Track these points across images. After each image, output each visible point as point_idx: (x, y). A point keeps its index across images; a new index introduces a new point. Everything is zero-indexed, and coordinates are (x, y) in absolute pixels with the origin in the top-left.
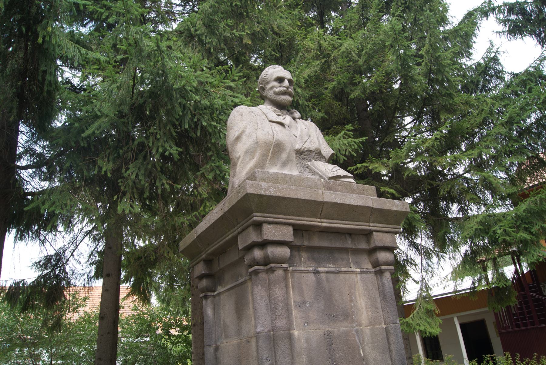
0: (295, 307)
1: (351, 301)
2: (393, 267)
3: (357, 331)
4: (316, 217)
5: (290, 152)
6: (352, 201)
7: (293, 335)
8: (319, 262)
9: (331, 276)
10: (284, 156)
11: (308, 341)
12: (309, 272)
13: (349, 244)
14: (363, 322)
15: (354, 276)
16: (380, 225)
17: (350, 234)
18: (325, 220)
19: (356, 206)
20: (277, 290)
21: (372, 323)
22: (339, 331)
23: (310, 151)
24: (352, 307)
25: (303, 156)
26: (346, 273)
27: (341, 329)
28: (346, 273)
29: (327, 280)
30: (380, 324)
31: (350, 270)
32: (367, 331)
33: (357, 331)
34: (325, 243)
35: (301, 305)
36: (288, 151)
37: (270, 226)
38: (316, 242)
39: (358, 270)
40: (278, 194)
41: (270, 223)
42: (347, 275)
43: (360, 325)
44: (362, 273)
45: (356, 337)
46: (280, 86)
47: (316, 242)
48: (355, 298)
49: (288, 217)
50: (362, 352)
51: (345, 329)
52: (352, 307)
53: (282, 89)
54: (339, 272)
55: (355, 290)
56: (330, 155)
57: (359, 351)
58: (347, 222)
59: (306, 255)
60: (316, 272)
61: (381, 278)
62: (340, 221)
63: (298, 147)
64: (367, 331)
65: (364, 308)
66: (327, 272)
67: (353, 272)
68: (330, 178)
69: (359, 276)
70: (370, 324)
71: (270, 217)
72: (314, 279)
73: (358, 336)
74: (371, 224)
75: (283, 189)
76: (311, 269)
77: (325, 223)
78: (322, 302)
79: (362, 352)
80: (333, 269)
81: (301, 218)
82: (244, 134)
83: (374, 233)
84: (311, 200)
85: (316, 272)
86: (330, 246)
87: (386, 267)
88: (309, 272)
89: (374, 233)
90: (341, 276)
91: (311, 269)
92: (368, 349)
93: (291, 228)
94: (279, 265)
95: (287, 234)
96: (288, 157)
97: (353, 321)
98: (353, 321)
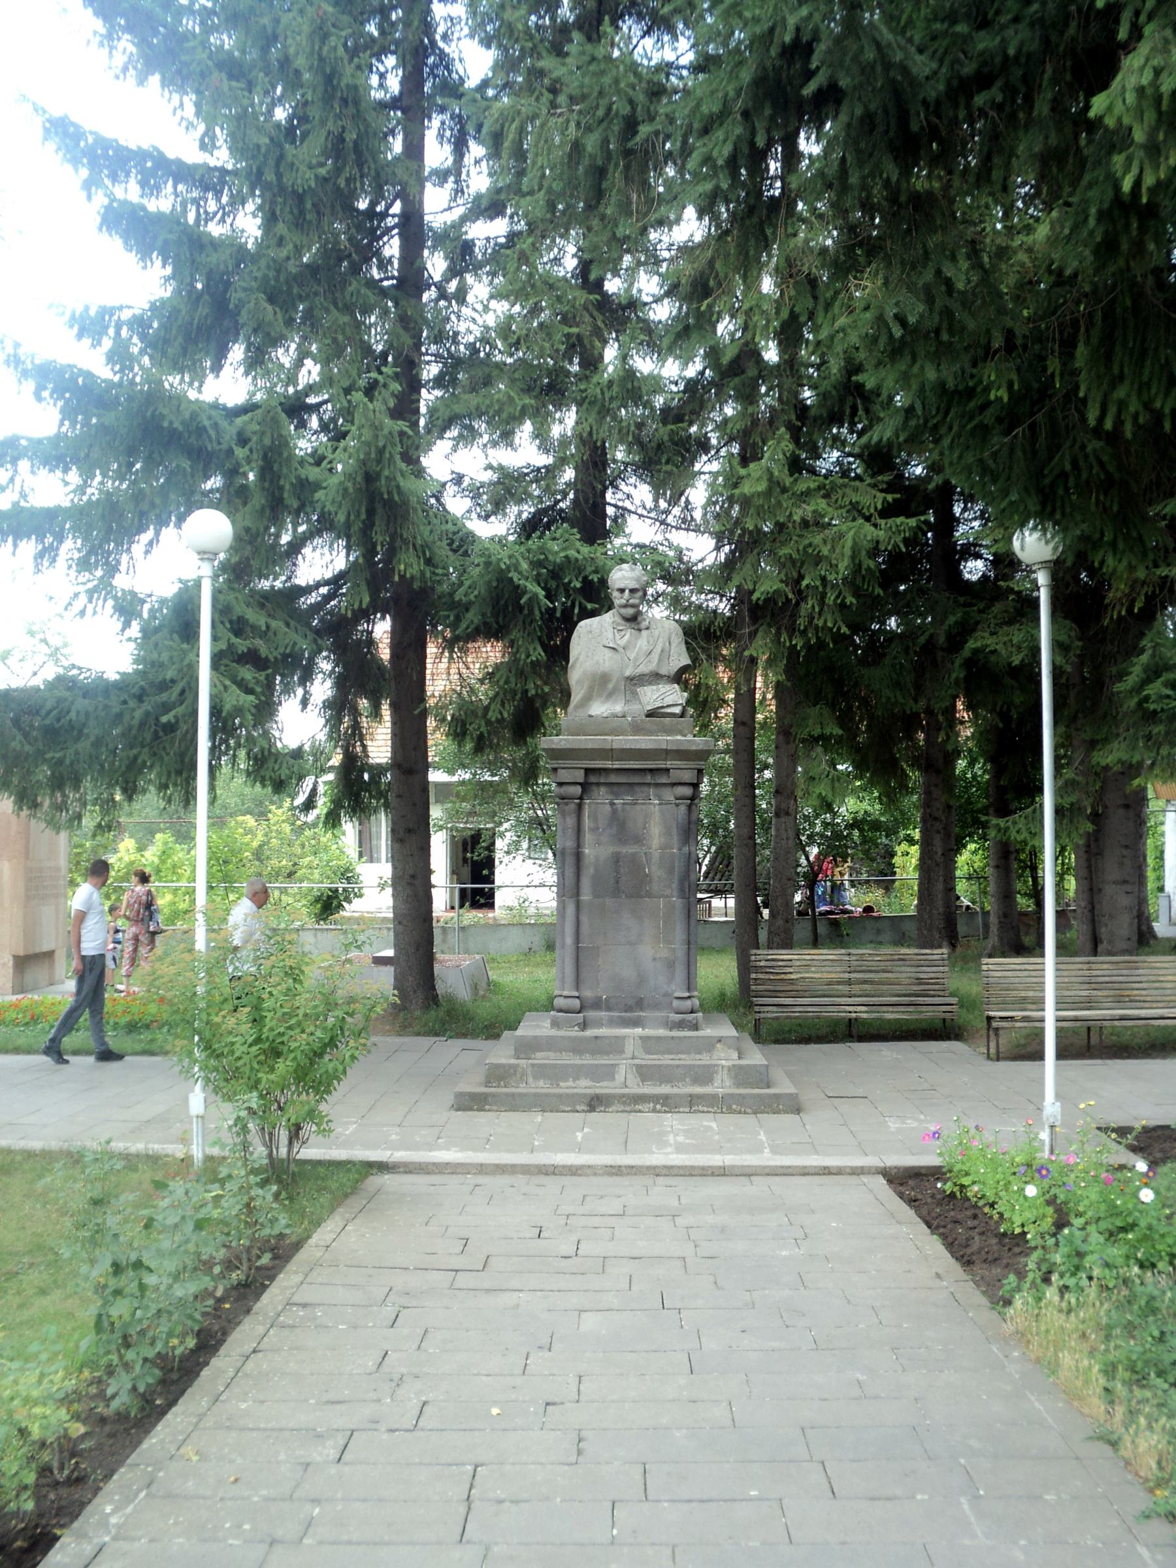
8: (617, 796)
10: (610, 686)
13: (648, 779)
21: (663, 847)
32: (656, 855)
35: (594, 830)
38: (613, 778)
47: (613, 778)
53: (623, 601)
60: (612, 804)
63: (628, 673)
77: (617, 765)
92: (654, 868)
95: (580, 776)
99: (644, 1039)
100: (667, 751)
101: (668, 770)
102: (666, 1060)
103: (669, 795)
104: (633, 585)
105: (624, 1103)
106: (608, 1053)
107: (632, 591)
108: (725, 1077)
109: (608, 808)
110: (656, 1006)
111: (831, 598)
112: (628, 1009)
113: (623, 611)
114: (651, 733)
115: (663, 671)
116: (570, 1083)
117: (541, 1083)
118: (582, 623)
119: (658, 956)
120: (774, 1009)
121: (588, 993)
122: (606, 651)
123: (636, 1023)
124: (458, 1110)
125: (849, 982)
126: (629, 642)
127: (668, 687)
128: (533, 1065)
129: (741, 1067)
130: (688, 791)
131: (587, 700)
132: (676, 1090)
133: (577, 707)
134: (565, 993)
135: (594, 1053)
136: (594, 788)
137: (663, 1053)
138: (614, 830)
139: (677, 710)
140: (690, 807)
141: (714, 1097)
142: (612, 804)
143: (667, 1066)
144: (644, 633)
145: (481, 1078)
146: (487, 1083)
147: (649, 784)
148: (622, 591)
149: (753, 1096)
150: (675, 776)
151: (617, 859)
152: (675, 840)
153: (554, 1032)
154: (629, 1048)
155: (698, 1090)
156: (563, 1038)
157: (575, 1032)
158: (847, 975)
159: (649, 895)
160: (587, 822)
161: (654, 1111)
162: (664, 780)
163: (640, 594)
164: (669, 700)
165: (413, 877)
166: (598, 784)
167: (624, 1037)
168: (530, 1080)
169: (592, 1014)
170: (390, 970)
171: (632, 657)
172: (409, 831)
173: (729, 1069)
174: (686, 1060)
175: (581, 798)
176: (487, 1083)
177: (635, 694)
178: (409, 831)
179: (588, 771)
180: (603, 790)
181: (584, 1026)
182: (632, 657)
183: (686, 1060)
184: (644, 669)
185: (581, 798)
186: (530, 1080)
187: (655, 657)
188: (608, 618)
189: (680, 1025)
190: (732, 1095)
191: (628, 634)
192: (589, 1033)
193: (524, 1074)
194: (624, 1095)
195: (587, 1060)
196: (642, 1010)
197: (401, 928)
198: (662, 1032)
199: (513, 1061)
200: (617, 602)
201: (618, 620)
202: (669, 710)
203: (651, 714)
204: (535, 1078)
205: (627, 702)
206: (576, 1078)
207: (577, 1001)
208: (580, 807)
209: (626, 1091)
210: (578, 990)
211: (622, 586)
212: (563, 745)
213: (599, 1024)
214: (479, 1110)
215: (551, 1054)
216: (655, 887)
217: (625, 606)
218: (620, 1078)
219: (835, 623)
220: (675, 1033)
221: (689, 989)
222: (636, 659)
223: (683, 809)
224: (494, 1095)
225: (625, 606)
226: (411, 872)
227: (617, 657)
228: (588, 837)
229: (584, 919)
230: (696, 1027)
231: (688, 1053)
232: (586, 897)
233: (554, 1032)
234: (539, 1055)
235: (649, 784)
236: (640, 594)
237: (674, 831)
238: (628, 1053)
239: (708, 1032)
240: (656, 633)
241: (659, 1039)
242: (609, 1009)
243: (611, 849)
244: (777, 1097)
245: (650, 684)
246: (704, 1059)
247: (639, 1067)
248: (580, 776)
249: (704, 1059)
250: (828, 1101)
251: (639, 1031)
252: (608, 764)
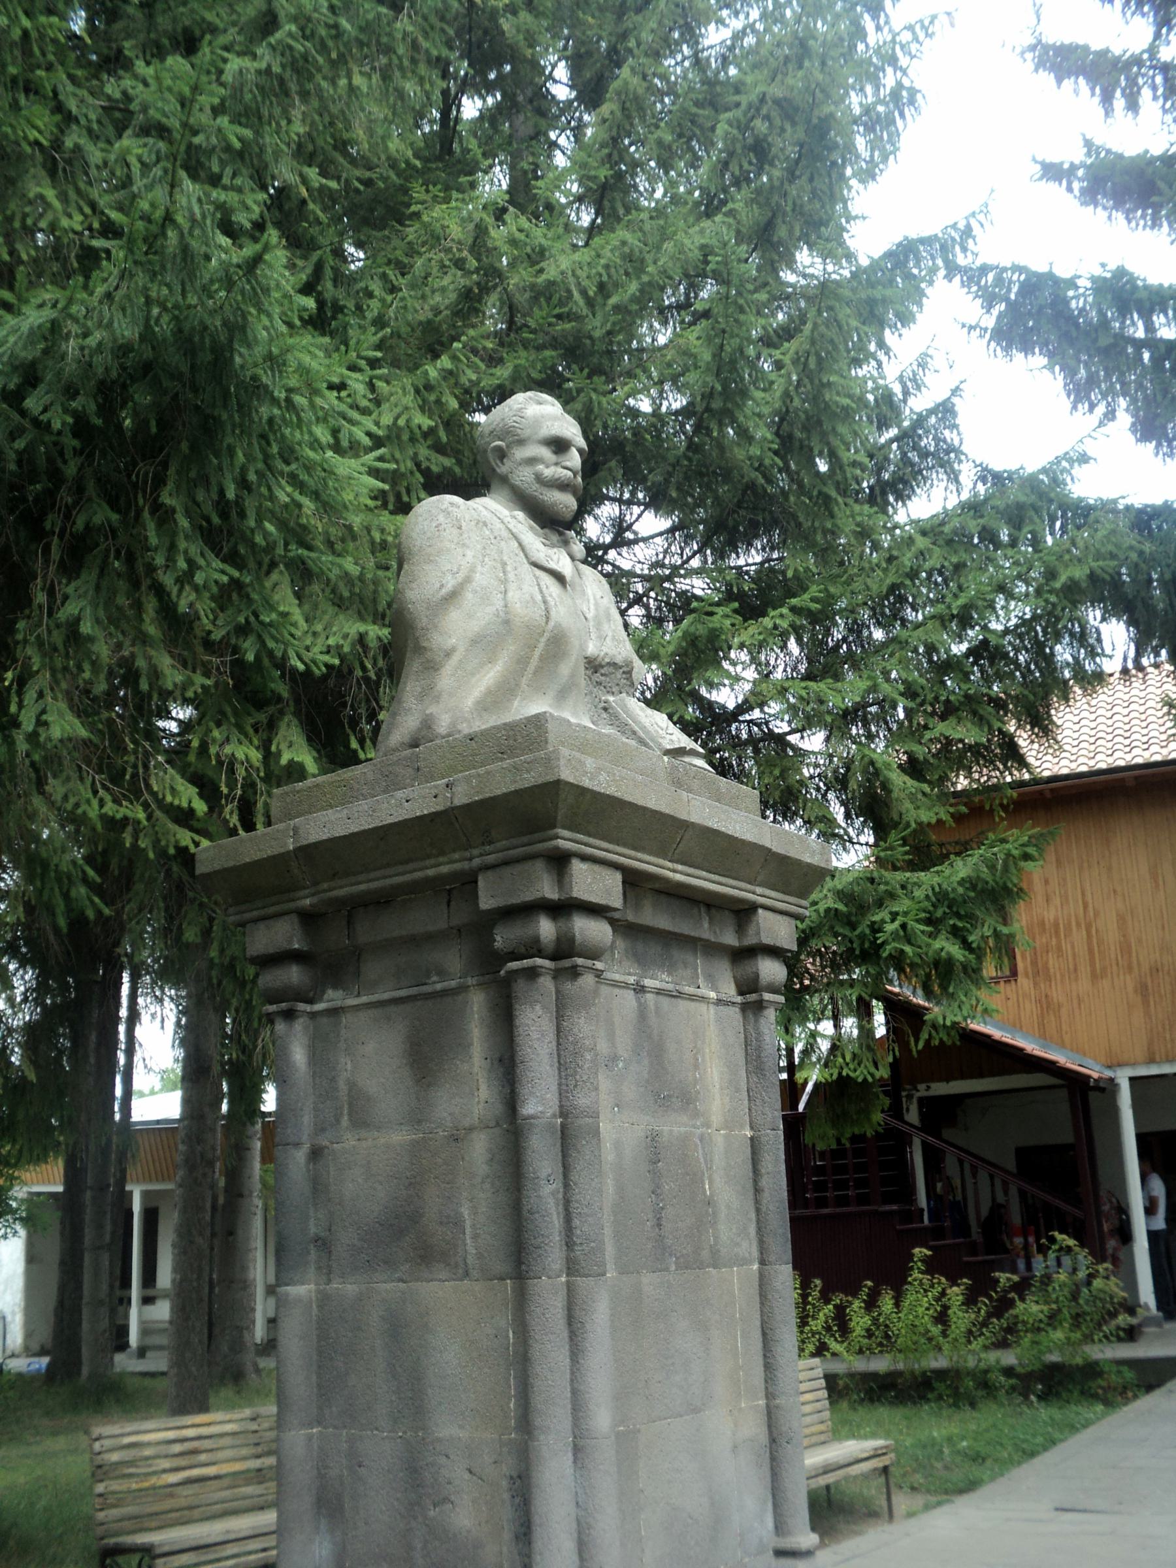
1: (696, 1067)
3: (702, 1138)
9: (665, 1001)
12: (626, 986)
13: (704, 930)
15: (703, 1007)
16: (773, 894)
17: (709, 906)
18: (680, 867)
19: (743, 842)
20: (582, 1021)
23: (615, 664)
24: (696, 1082)
25: (597, 677)
28: (692, 998)
30: (742, 1127)
31: (699, 992)
33: (702, 1138)
39: (713, 995)
40: (611, 791)
41: (584, 858)
44: (719, 1002)
46: (556, 464)
51: (683, 1129)
52: (696, 1082)
54: (679, 995)
57: (703, 1183)
58: (712, 877)
60: (640, 989)
61: (756, 1021)
63: (592, 649)
64: (719, 1139)
66: (659, 992)
67: (703, 999)
68: (668, 752)
69: (712, 1007)
71: (586, 844)
72: (634, 1003)
74: (759, 890)
75: (623, 778)
78: (646, 1062)
80: (670, 987)
82: (470, 587)
83: (760, 911)
85: (640, 989)
86: (671, 929)
88: (626, 986)
89: (760, 911)
90: (683, 1004)
91: (631, 980)
93: (618, 876)
94: (589, 963)
96: (572, 676)
97: (696, 1114)
98: (696, 1114)
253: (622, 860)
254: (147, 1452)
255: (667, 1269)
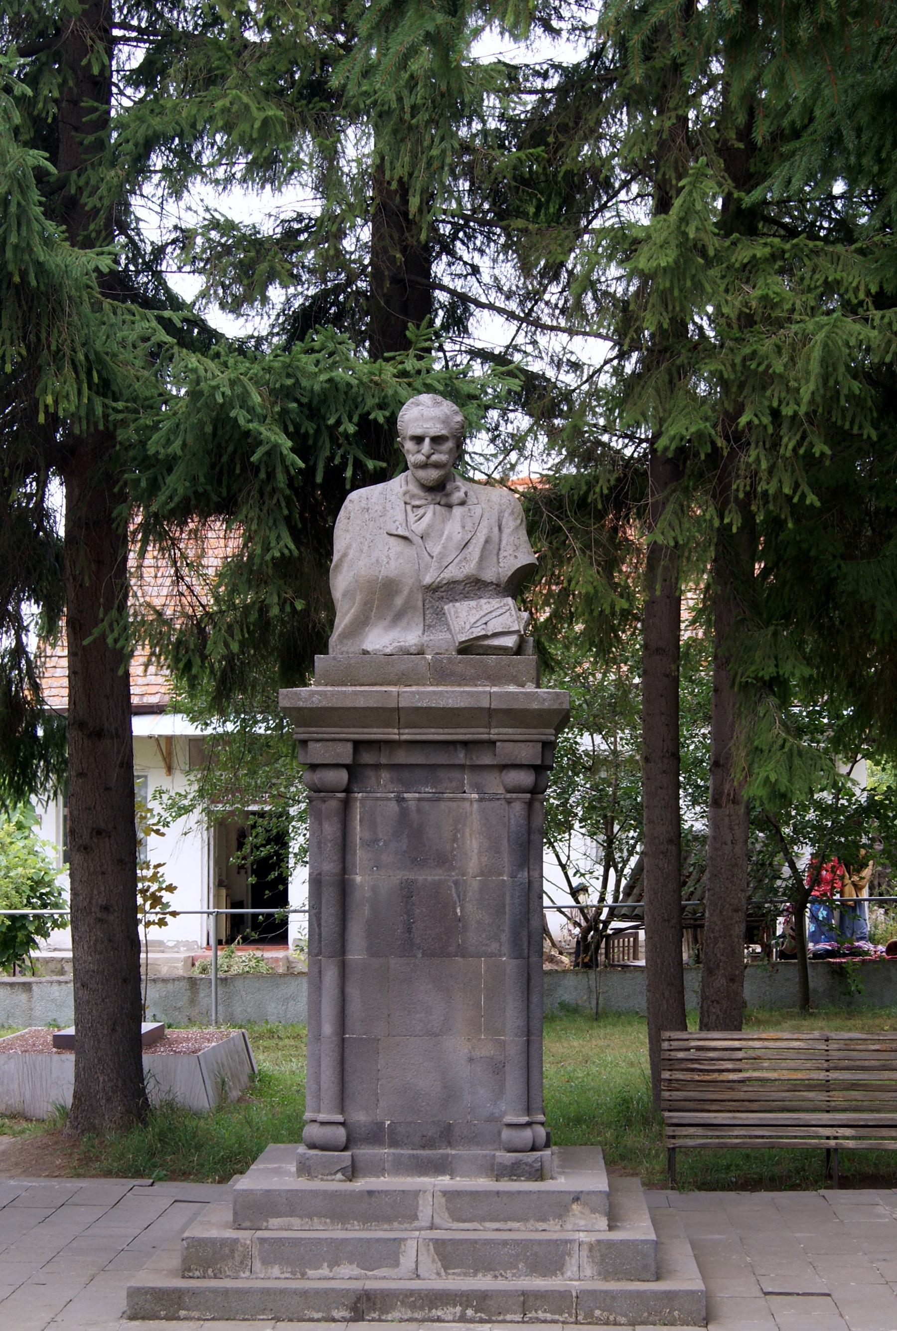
0: (362, 846)
1: (455, 840)
2: (529, 795)
3: (456, 883)
4: (393, 727)
5: (411, 591)
6: (450, 701)
7: (354, 880)
9: (426, 805)
10: (399, 601)
11: (375, 889)
13: (461, 757)
14: (471, 871)
21: (485, 872)
22: (426, 880)
23: (454, 582)
24: (453, 849)
26: (451, 799)
27: (430, 878)
28: (451, 799)
29: (419, 811)
30: (501, 874)
32: (475, 884)
33: (456, 883)
34: (417, 758)
35: (370, 843)
36: (405, 593)
37: (318, 745)
38: (402, 757)
40: (324, 704)
41: (318, 740)
42: (455, 804)
43: (464, 875)
45: (453, 890)
47: (402, 757)
48: (463, 836)
49: (345, 730)
50: (458, 910)
51: (437, 878)
52: (453, 849)
53: (421, 458)
55: (464, 825)
56: (510, 573)
57: (455, 909)
58: (446, 730)
59: (388, 776)
60: (400, 800)
62: (433, 730)
63: (428, 580)
65: (476, 851)
66: (419, 800)
67: (464, 799)
70: (482, 874)
72: (397, 808)
73: (457, 889)
76: (392, 795)
77: (407, 735)
78: (405, 841)
79: (458, 910)
81: (366, 730)
83: (498, 744)
84: (376, 708)
87: (514, 795)
88: (390, 799)
92: (470, 907)
93: (350, 746)
95: (345, 753)
97: (452, 868)
99: (450, 1195)
100: (490, 713)
101: (493, 743)
102: (488, 1231)
103: (495, 784)
104: (436, 429)
105: (413, 1307)
106: (389, 1220)
107: (437, 440)
108: (585, 1261)
109: (393, 806)
110: (473, 1139)
111: (789, 443)
112: (428, 1143)
113: (421, 474)
114: (462, 680)
115: (489, 575)
116: (325, 1271)
117: (276, 1271)
118: (354, 495)
119: (477, 1054)
120: (700, 1131)
121: (360, 1117)
122: (392, 540)
123: (440, 1167)
124: (132, 1318)
125: (826, 1086)
126: (430, 526)
127: (495, 603)
128: (262, 1240)
129: (610, 1244)
130: (526, 778)
131: (361, 624)
132: (500, 1284)
133: (344, 636)
134: (322, 1117)
135: (367, 1219)
136: (370, 773)
137: (482, 1220)
138: (404, 844)
139: (510, 641)
140: (530, 805)
141: (564, 1295)
142: (400, 800)
143: (487, 1242)
144: (458, 511)
145: (175, 1262)
146: (185, 1272)
147: (462, 767)
148: (419, 440)
149: (630, 1294)
150: (506, 752)
151: (408, 891)
152: (506, 860)
153: (303, 1184)
154: (425, 1211)
155: (539, 1283)
156: (314, 1193)
157: (337, 1184)
158: (822, 1075)
159: (462, 952)
160: (358, 830)
161: (463, 1319)
162: (487, 760)
163: (450, 444)
164: (496, 626)
165: (106, 909)
166: (377, 767)
167: (416, 1193)
168: (257, 1265)
169: (365, 1152)
170: (70, 1058)
171: (436, 550)
172: (99, 832)
173: (591, 1247)
174: (521, 1232)
175: (348, 790)
176: (185, 1272)
177: (440, 615)
178: (98, 832)
179: (358, 745)
180: (385, 775)
181: (353, 1172)
182: (436, 550)
183: (521, 1232)
184: (454, 572)
185: (348, 790)
186: (257, 1265)
187: (475, 551)
188: (397, 485)
189: (513, 1172)
190: (593, 1293)
191: (430, 513)
192: (361, 1184)
193: (246, 1257)
194: (412, 1293)
195: (356, 1232)
196: (450, 1144)
197: (85, 994)
198: (483, 1183)
199: (230, 1234)
200: (411, 459)
201: (414, 489)
202: (496, 642)
203: (467, 648)
204: (266, 1262)
205: (427, 628)
206: (334, 1263)
207: (341, 1132)
208: (346, 805)
209: (416, 1285)
210: (342, 1111)
211: (418, 432)
212: (316, 702)
213: (378, 1169)
214: (168, 1318)
215: (296, 1221)
216: (473, 938)
217: (424, 466)
218: (407, 1261)
219: (796, 486)
220: (505, 1185)
221: (528, 1111)
222: (442, 556)
223: (518, 808)
224: (194, 1293)
225: (424, 466)
226: (102, 901)
227: (408, 552)
228: (360, 856)
229: (353, 992)
230: (539, 1174)
231: (524, 1219)
232: (356, 954)
233: (303, 1184)
234: (274, 1222)
235: (462, 767)
236: (450, 444)
237: (505, 845)
238: (424, 1220)
239: (561, 1183)
240: (478, 510)
241: (474, 1195)
242: (394, 1144)
243: (399, 876)
244: (670, 1296)
245: (466, 597)
246: (552, 1231)
247: (440, 1245)
248: (345, 753)
249: (552, 1231)
250: (762, 1302)
251: (444, 1181)
252: (393, 734)
253: (349, 736)
254: (711, 1054)
255: (415, 956)
